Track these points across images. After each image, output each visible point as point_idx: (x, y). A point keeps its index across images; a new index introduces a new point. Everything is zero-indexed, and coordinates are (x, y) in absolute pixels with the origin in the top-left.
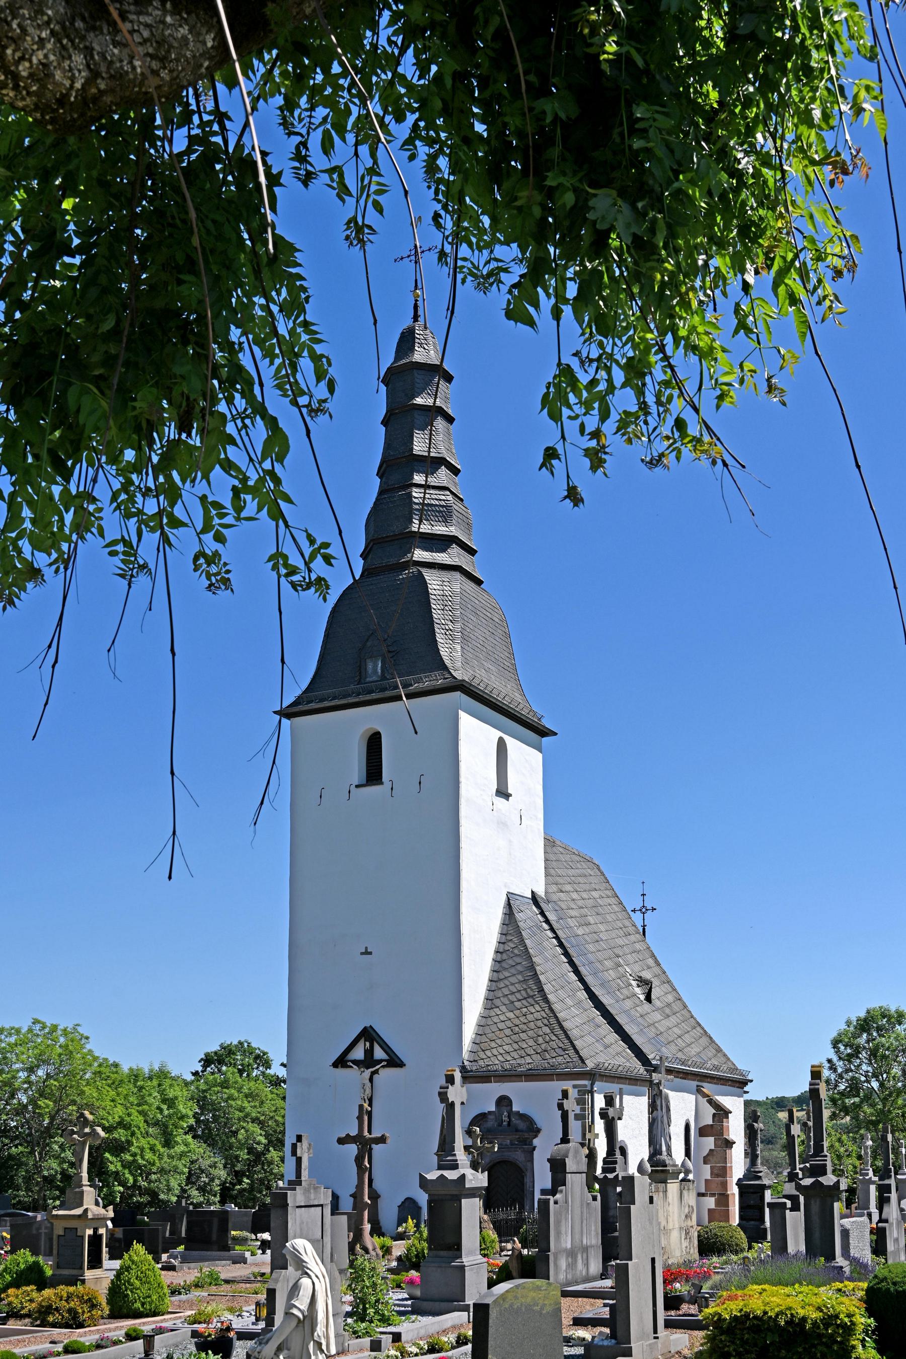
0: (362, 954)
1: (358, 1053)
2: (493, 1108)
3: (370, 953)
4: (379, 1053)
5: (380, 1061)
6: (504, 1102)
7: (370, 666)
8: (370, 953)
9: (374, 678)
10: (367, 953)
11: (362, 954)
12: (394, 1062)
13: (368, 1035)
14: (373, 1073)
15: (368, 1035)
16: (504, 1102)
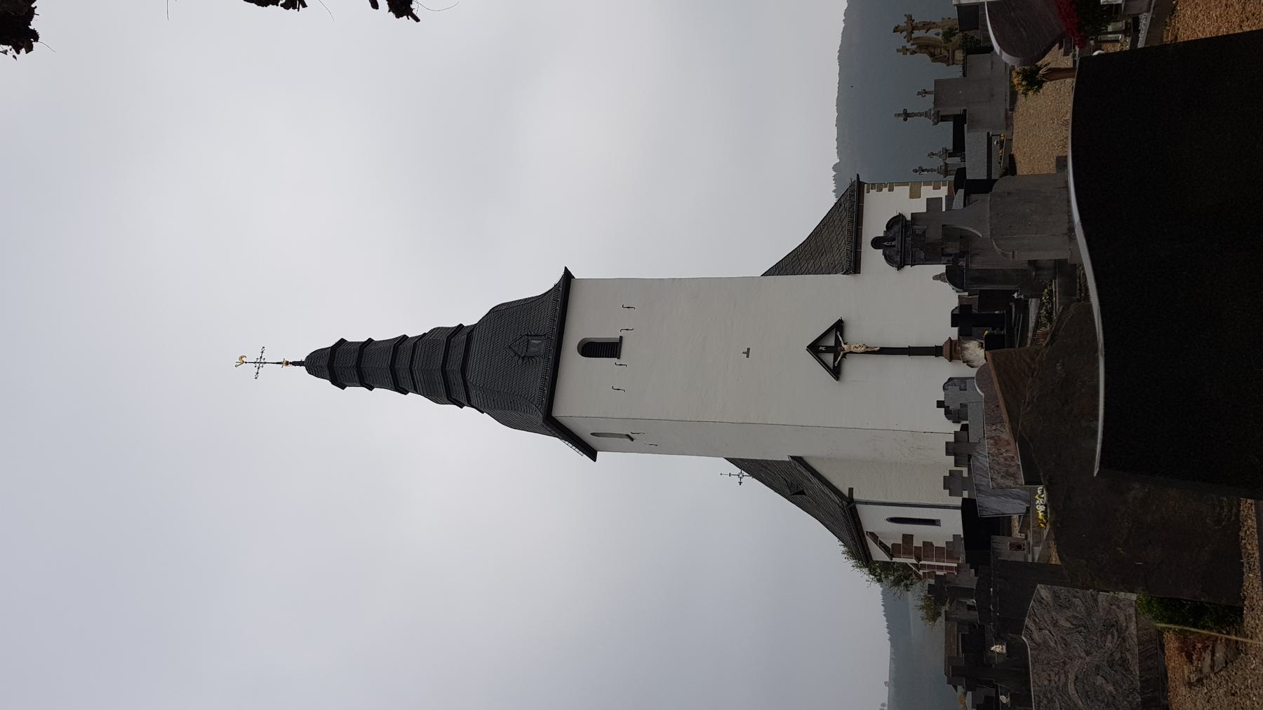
0: (748, 357)
1: (829, 358)
2: (881, 251)
3: (749, 349)
4: (831, 342)
5: (837, 338)
6: (876, 243)
7: (532, 349)
8: (749, 349)
9: (543, 346)
10: (747, 353)
11: (748, 357)
12: (839, 326)
13: (814, 348)
14: (845, 344)
15: (814, 348)
16: (876, 243)
